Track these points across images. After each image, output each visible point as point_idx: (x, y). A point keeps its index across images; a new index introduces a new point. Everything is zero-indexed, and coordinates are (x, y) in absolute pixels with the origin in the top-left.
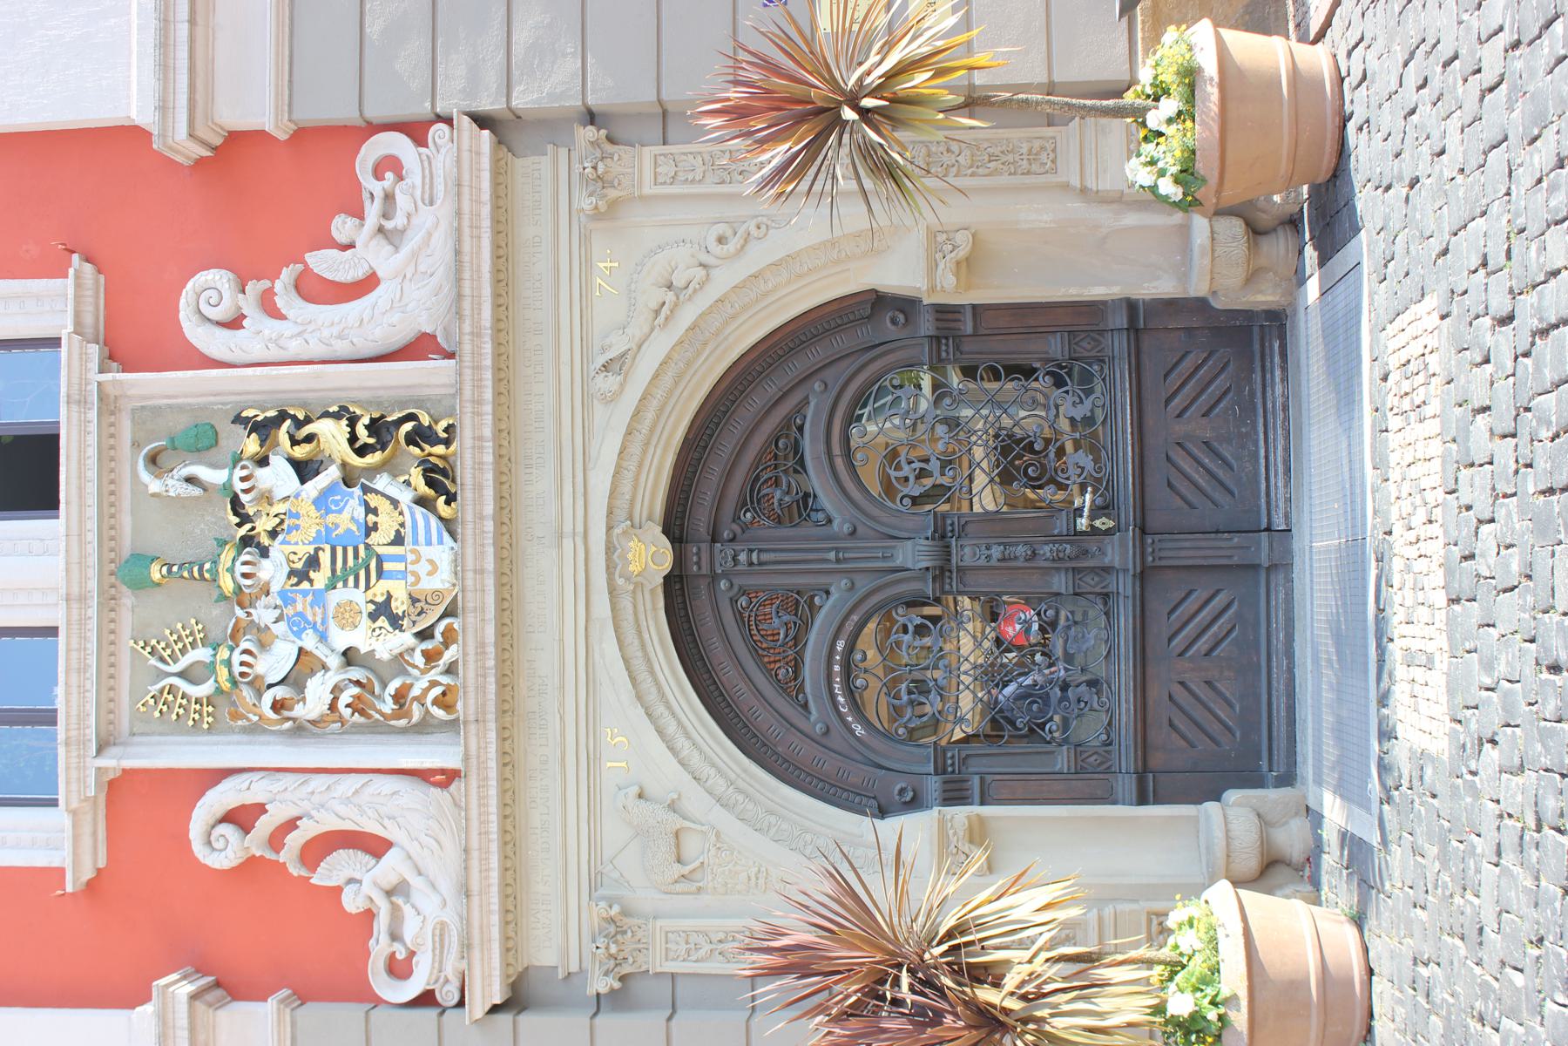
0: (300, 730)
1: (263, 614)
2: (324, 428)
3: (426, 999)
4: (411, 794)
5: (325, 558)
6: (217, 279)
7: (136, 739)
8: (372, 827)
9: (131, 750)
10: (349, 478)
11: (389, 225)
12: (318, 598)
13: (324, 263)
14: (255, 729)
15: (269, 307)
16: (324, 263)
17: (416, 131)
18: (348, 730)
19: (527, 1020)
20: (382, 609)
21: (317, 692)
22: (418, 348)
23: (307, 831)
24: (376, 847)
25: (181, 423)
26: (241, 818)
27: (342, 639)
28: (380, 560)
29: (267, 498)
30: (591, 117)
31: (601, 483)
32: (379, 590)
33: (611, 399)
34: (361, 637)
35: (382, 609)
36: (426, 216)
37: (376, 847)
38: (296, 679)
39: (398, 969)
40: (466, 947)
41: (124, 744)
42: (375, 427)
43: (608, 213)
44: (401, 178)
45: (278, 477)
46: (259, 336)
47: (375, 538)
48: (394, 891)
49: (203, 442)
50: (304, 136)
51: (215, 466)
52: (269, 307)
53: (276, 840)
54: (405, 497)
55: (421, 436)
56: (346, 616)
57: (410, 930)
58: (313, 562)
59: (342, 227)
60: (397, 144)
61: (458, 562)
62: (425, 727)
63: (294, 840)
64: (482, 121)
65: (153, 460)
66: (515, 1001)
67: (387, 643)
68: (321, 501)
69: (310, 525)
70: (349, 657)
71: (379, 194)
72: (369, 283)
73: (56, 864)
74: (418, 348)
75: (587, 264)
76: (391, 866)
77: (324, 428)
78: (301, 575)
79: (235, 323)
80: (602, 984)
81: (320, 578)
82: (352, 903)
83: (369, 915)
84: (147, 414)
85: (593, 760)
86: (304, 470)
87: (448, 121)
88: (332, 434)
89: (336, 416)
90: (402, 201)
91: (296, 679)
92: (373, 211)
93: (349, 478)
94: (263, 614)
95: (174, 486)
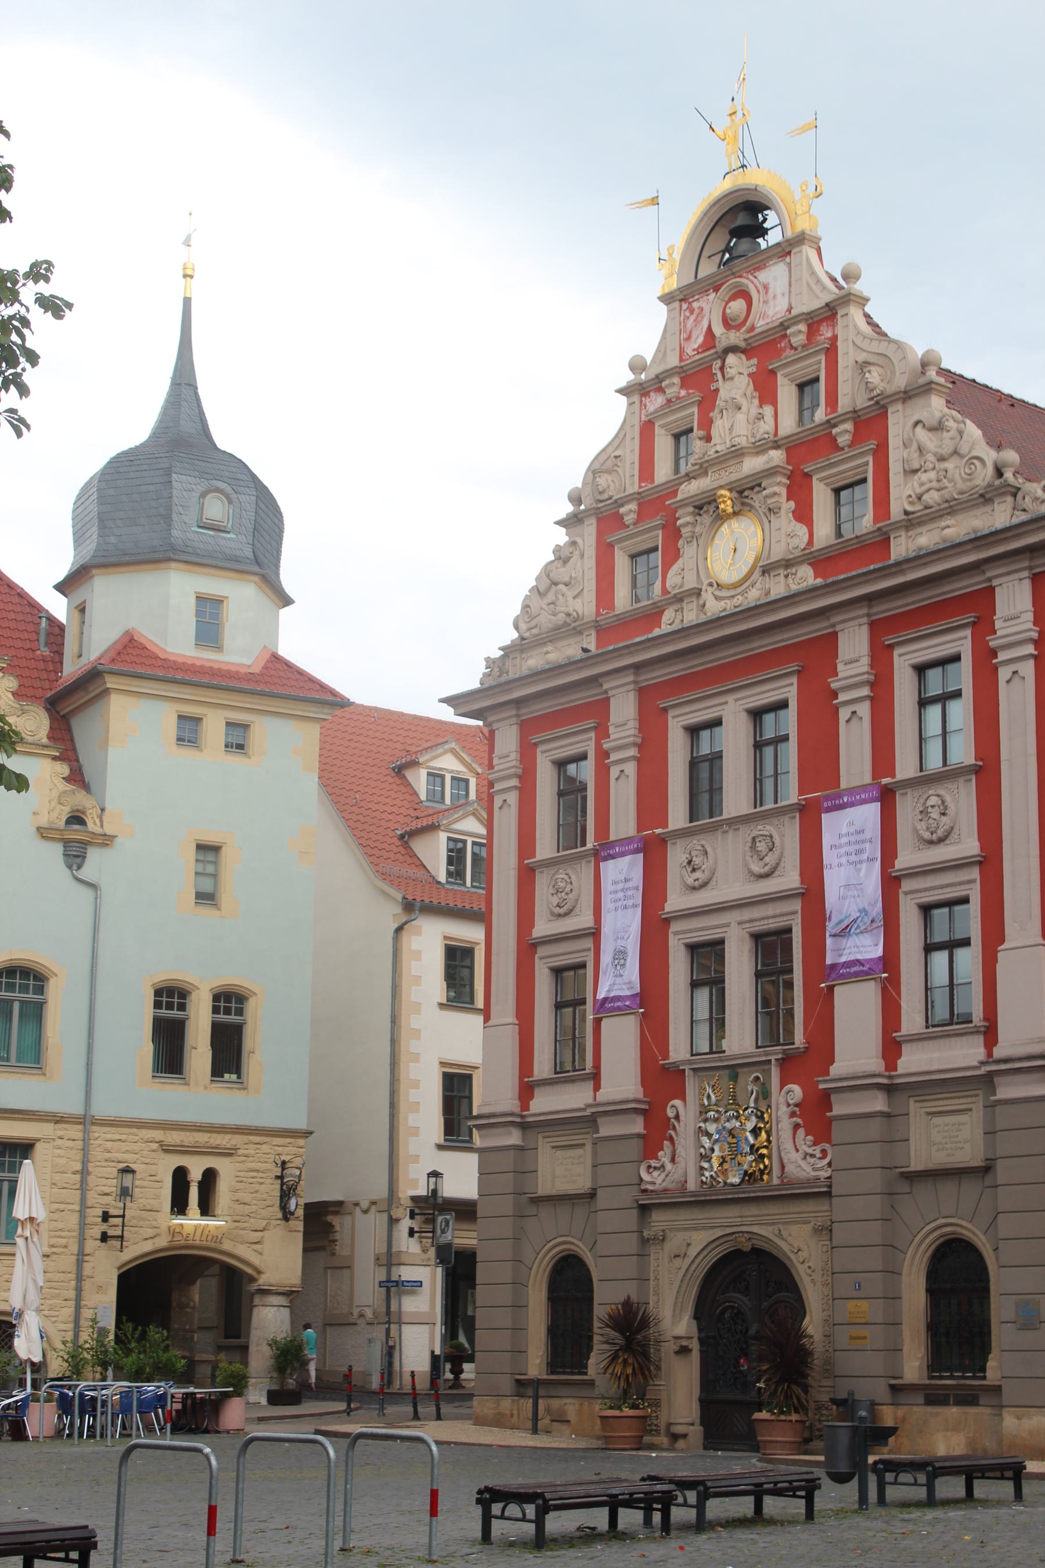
2: (764, 1135)
5: (734, 1141)
7: (696, 1079)
9: (692, 1079)
10: (752, 1146)
11: (808, 1157)
13: (801, 1132)
15: (793, 1114)
16: (801, 1132)
24: (673, 1160)
26: (677, 1117)
27: (716, 1148)
28: (734, 1159)
32: (728, 1159)
34: (717, 1153)
36: (809, 1169)
37: (673, 1160)
41: (694, 1076)
42: (762, 1156)
44: (820, 1158)
45: (750, 1125)
47: (739, 1156)
48: (663, 1166)
51: (756, 1101)
54: (746, 1167)
58: (734, 1137)
63: (672, 1132)
64: (830, 1186)
65: (757, 1078)
70: (712, 1150)
71: (814, 1153)
73: (671, 1054)
76: (669, 1166)
78: (731, 1133)
79: (789, 1105)
81: (730, 1139)
82: (661, 1153)
86: (756, 1132)
87: (830, 1178)
89: (769, 1141)
90: (812, 1160)
95: (750, 1088)
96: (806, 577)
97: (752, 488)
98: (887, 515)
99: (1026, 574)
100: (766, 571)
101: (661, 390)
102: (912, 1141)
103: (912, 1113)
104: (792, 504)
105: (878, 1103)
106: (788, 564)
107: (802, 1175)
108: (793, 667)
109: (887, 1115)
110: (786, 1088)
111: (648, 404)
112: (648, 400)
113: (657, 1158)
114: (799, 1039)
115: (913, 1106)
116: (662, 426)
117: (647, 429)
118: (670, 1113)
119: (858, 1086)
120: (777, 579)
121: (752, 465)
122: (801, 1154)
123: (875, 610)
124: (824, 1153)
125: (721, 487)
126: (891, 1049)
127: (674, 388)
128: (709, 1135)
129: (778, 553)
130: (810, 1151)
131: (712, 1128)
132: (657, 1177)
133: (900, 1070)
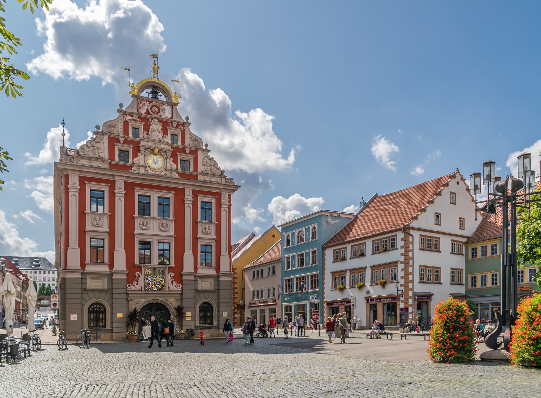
0: (144, 280)
1: (152, 277)
2: (164, 282)
3: (127, 287)
4: (141, 287)
6: (173, 276)
8: (138, 285)
12: (153, 281)
13: (174, 282)
14: (144, 277)
15: (171, 278)
16: (174, 282)
17: (182, 288)
18: (144, 283)
19: (126, 294)
20: (152, 285)
21: (147, 281)
22: (169, 288)
23: (138, 280)
24: (137, 285)
25: (164, 272)
26: (139, 276)
27: (150, 283)
29: (159, 278)
30: (182, 299)
31: (160, 299)
33: (165, 300)
34: (150, 284)
35: (152, 285)
37: (137, 285)
38: (148, 280)
39: (129, 286)
40: (130, 290)
43: (176, 300)
45: (161, 279)
46: (170, 277)
49: (163, 274)
50: (182, 280)
52: (171, 278)
53: (137, 278)
55: (163, 288)
56: (152, 283)
57: (131, 287)
59: (176, 283)
60: (181, 287)
61: (155, 290)
62: (145, 288)
64: (182, 292)
66: (127, 294)
67: (150, 286)
68: (159, 282)
69: (157, 281)
70: (149, 283)
72: (173, 285)
74: (169, 288)
75: (173, 298)
77: (164, 282)
79: (171, 276)
80: (128, 299)
83: (132, 284)
84: (165, 270)
85: (142, 298)
86: (161, 281)
88: (163, 282)
91: (148, 280)
92: (177, 285)
93: (161, 283)
94: (152, 277)
96: (175, 175)
97: (162, 151)
98: (197, 171)
99: (228, 193)
100: (165, 170)
101: (132, 116)
102: (199, 285)
103: (199, 280)
104: (172, 159)
105: (193, 278)
106: (172, 170)
107: (174, 290)
108: (109, 185)
109: (195, 280)
110: (170, 274)
111: (126, 117)
112: (126, 116)
113: (132, 284)
114: (172, 264)
115: (199, 279)
116: (130, 124)
117: (126, 123)
118: (137, 274)
119: (189, 274)
120: (169, 173)
121: (162, 146)
122: (174, 286)
123: (195, 188)
124: (180, 286)
125: (156, 148)
126: (196, 268)
127: (136, 118)
128: (149, 280)
129: (169, 167)
130: (177, 285)
131: (149, 279)
132: (133, 288)
133: (198, 273)
